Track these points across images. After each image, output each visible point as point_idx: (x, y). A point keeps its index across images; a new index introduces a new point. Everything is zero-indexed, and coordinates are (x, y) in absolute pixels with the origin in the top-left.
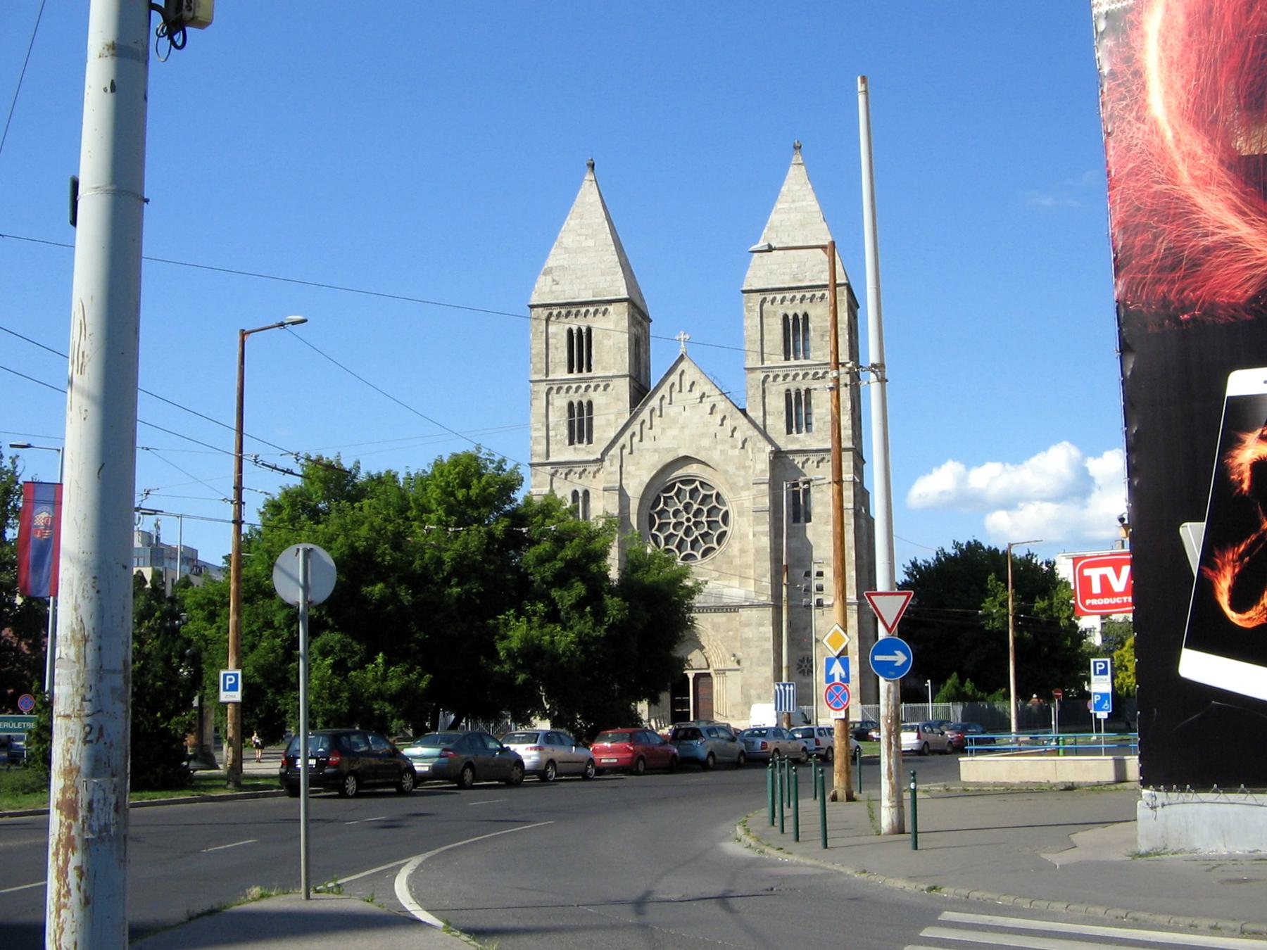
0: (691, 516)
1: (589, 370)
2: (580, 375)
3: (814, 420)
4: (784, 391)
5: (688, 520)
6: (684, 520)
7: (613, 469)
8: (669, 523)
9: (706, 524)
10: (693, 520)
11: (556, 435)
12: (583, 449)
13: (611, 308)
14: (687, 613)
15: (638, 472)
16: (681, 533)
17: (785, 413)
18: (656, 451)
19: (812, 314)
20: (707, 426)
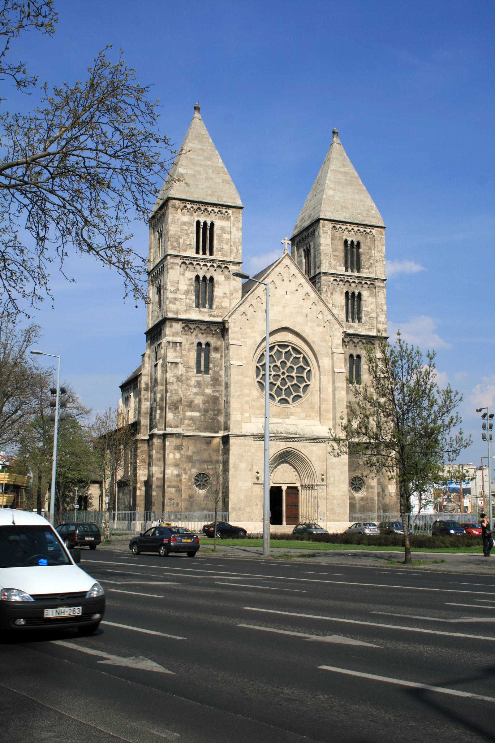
0: (285, 371)
1: (211, 254)
2: (205, 257)
3: (363, 315)
4: (344, 292)
5: (283, 373)
6: (280, 373)
9: (295, 378)
10: (287, 374)
11: (186, 299)
12: (206, 312)
13: (230, 212)
16: (278, 383)
17: (345, 307)
20: (301, 308)
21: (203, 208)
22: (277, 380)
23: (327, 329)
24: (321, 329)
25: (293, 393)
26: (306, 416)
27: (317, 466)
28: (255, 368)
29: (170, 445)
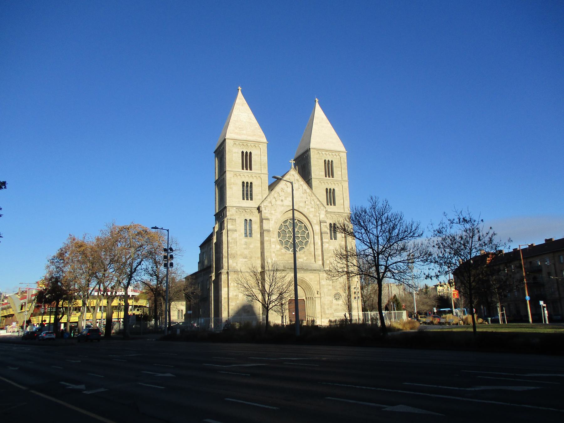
7: (266, 211)
14: (128, 274)
15: (276, 214)
18: (283, 206)
22: (290, 239)
23: (317, 209)
24: (313, 210)
25: (299, 246)
27: (315, 287)
28: (277, 233)
29: (231, 278)
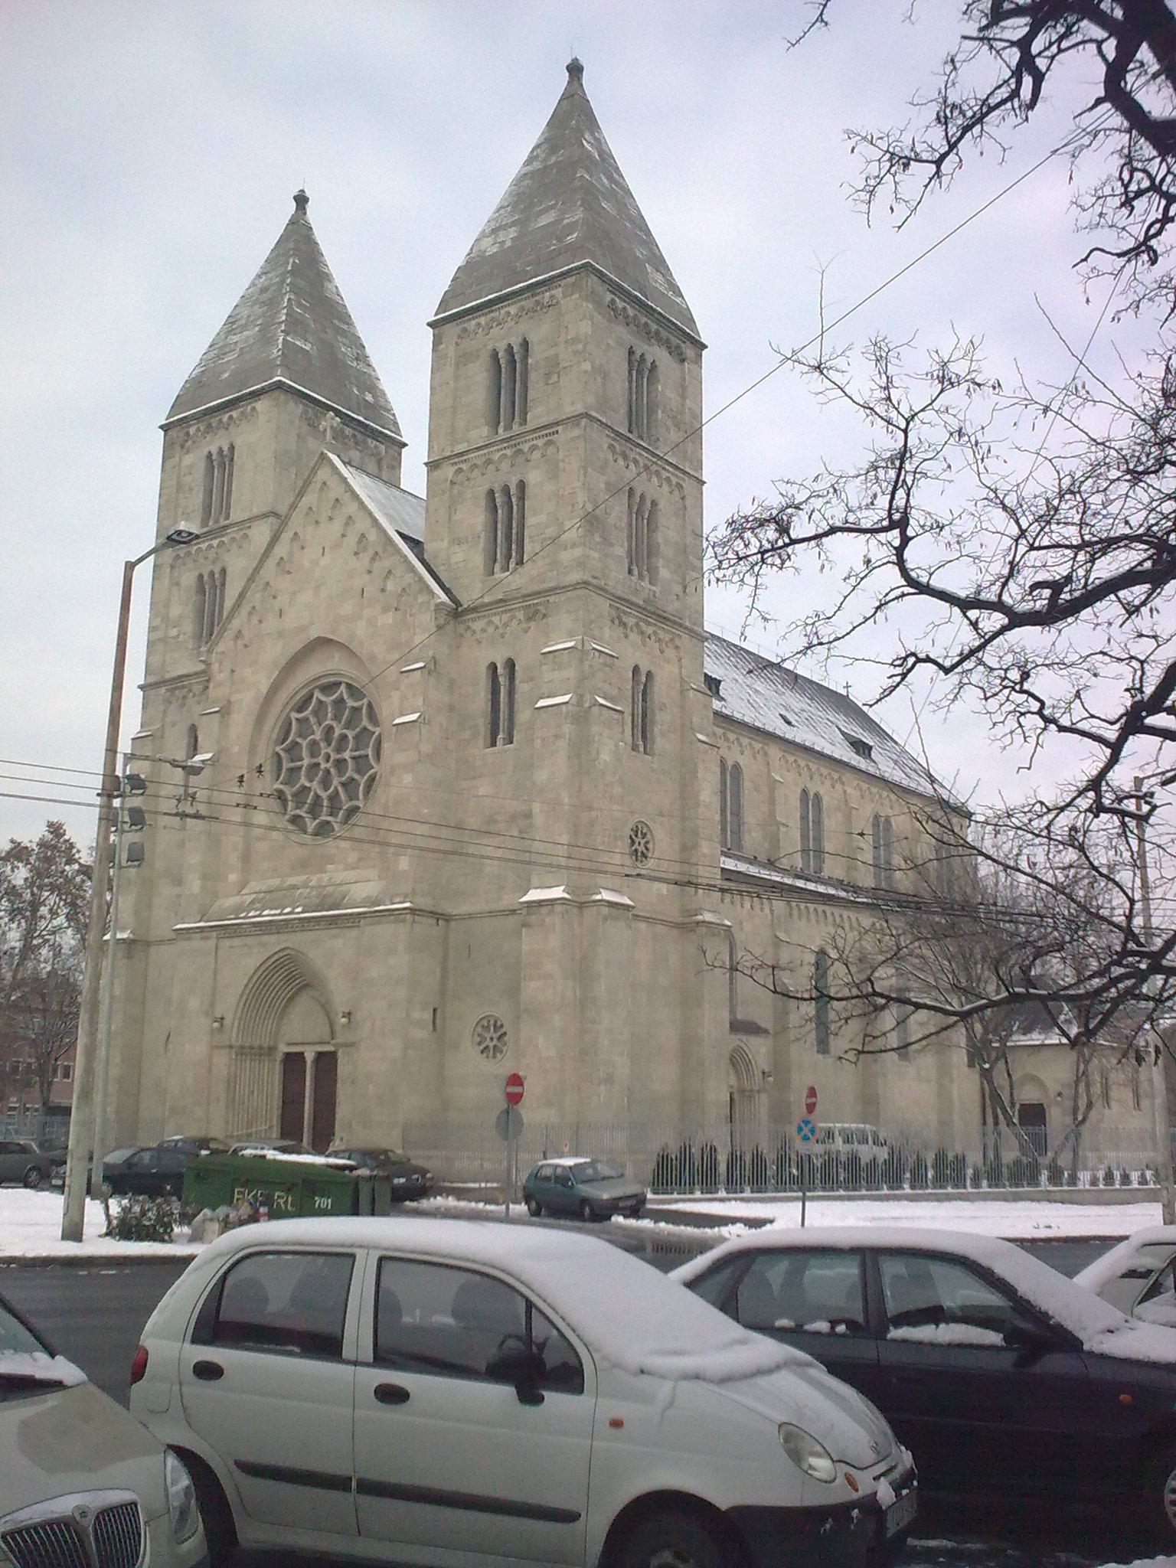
8: (300, 768)
9: (349, 760)
19: (533, 338)
21: (214, 422)
26: (360, 859)
